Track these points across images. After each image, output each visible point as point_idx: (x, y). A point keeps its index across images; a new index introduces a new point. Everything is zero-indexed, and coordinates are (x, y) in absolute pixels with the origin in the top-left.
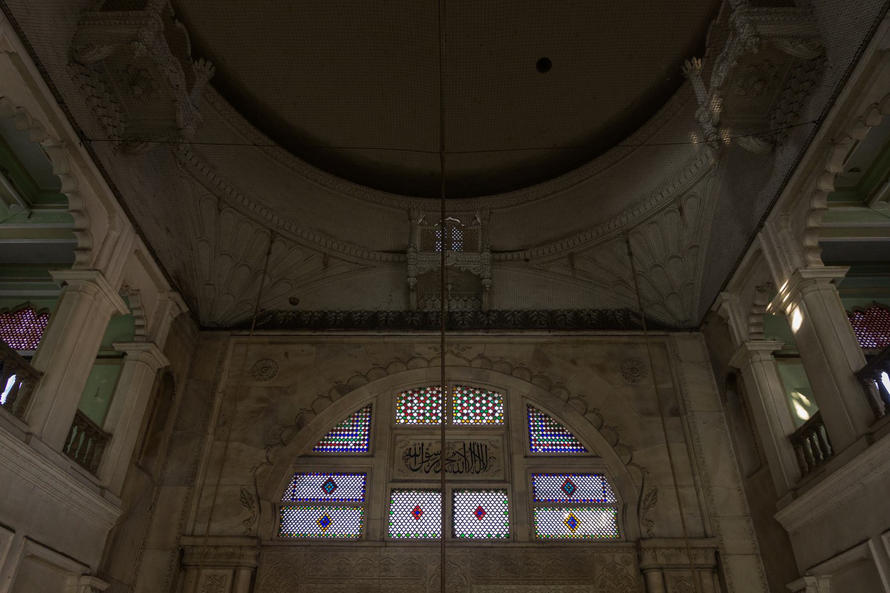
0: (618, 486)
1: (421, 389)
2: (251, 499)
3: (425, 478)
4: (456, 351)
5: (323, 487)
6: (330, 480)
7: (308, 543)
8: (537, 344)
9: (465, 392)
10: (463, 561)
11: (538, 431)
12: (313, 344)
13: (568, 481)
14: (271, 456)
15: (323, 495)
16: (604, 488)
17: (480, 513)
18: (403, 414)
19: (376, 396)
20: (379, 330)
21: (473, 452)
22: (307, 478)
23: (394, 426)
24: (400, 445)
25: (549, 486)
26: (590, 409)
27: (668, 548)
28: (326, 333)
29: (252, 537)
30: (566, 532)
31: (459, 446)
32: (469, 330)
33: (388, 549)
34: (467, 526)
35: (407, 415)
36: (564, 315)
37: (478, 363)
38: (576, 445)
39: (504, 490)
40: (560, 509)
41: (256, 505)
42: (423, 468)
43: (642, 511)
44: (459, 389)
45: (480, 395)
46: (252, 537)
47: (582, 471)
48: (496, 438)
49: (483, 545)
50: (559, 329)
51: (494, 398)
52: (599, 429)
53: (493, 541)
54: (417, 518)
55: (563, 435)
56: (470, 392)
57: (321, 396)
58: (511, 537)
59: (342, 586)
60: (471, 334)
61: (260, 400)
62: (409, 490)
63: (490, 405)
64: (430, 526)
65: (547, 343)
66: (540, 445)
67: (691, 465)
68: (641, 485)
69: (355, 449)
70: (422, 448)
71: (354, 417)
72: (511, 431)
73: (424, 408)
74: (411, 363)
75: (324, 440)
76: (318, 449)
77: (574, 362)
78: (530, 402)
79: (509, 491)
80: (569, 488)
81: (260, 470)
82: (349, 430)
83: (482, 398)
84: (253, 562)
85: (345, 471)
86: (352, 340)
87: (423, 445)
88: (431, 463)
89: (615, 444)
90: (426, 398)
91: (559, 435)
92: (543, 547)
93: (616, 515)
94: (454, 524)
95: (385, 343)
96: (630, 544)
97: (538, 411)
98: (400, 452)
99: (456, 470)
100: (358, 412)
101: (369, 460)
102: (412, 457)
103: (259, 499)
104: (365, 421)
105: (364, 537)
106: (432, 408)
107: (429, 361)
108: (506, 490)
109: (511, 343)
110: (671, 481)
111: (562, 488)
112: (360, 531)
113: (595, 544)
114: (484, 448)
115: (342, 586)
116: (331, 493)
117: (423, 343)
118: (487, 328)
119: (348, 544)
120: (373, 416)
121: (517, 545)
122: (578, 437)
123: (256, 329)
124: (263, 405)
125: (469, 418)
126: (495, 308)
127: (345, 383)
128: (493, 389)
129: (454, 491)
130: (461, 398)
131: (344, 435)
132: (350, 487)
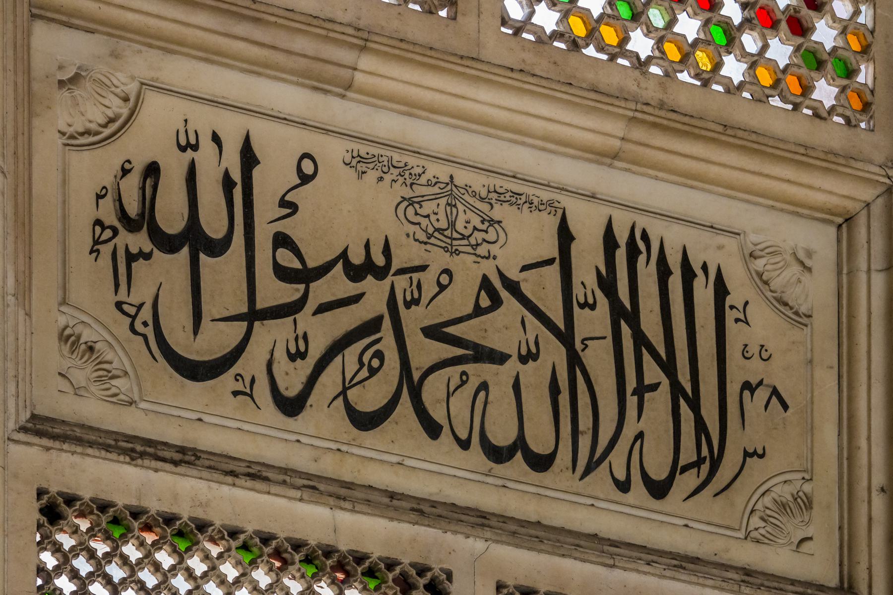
21: (624, 315)
24: (67, 113)
31: (524, 239)
42: (252, 364)
62: (183, 532)
70: (240, 186)
87: (249, 158)
88: (321, 331)
99: (502, 433)
102: (168, 243)
114: (704, 294)
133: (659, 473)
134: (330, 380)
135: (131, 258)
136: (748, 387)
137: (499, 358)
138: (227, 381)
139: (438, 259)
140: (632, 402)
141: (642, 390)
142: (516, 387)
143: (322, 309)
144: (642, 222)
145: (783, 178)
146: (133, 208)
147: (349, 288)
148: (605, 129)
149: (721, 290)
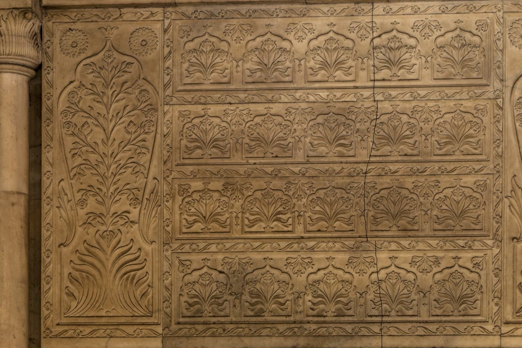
59: (276, 108)
84: (28, 51)
115: (276, 108)
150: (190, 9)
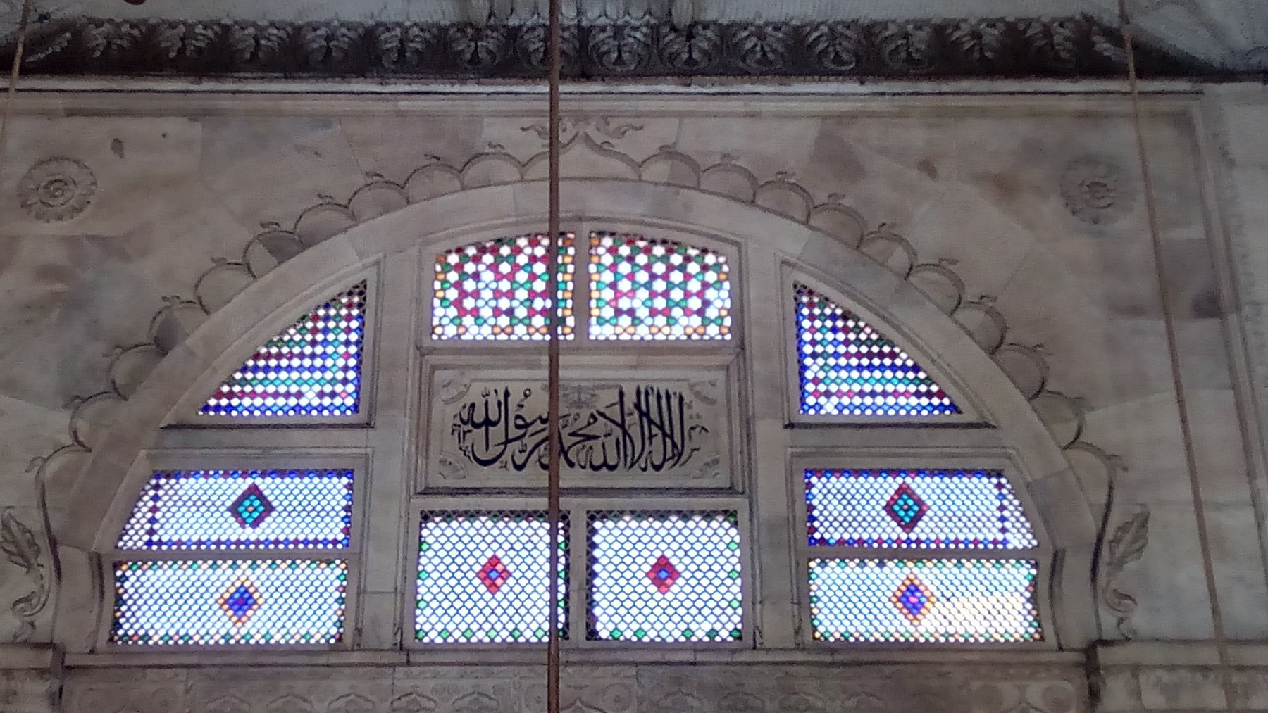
0: (1041, 505)
1: (500, 242)
2: (32, 543)
3: (513, 484)
4: (598, 138)
5: (234, 510)
6: (254, 490)
7: (193, 660)
8: (824, 117)
9: (625, 250)
10: (617, 700)
11: (824, 355)
12: (194, 116)
13: (903, 490)
14: (83, 426)
15: (233, 531)
16: (1002, 508)
17: (663, 573)
18: (453, 312)
19: (377, 263)
20: (383, 78)
21: (644, 414)
22: (188, 486)
23: (426, 343)
25: (850, 503)
26: (969, 296)
27: (1172, 668)
28: (229, 86)
29: (40, 646)
30: (894, 625)
32: (637, 76)
33: (415, 670)
34: (628, 608)
35: (463, 312)
36: (906, 36)
37: (659, 170)
38: (929, 395)
39: (729, 514)
40: (881, 565)
41: (46, 559)
42: (507, 457)
43: (1103, 569)
44: (608, 242)
45: (665, 259)
46: (40, 646)
47: (942, 464)
48: (708, 376)
49: (670, 657)
50: (891, 76)
51: (705, 268)
52: (993, 351)
53: (699, 647)
54: (493, 588)
55: (893, 368)
56: (640, 250)
57: (221, 263)
58: (747, 638)
60: (641, 88)
61: (47, 273)
63: (694, 286)
64: (526, 613)
65: (852, 116)
66: (828, 394)
67: (1247, 449)
68: (1104, 500)
69: (321, 408)
71: (316, 318)
72: (752, 360)
73: (510, 295)
74: (474, 171)
75: (231, 382)
76: (217, 408)
77: (928, 168)
78: (804, 279)
79: (743, 517)
80: (906, 510)
81: (53, 466)
82: (302, 356)
83: (671, 268)
85: (294, 465)
86: (308, 104)
87: (507, 394)
88: (530, 442)
89: (1037, 392)
90: (516, 268)
91: (882, 368)
92: (832, 664)
93: (1034, 581)
94: (591, 604)
95: (401, 114)
96: (1068, 657)
97: (826, 301)
98: (445, 414)
99: (597, 463)
100: (327, 306)
101: (361, 434)
102: (477, 426)
103: (54, 544)
104: (348, 330)
105: (348, 640)
106: (532, 295)
107: (523, 166)
108: (734, 514)
109: (752, 115)
110: (1186, 492)
111: (889, 508)
112: (340, 624)
113: (975, 657)
114: (675, 402)
116: (256, 524)
117: (502, 114)
118: (688, 71)
119: (305, 659)
120: (369, 317)
121: (762, 657)
122: (935, 373)
123: (25, 72)
124: (59, 287)
125: (636, 321)
126: (711, 15)
127: (288, 225)
128: (704, 242)
129: (593, 518)
130: (613, 267)
131: (289, 369)
132: (311, 506)
133: (657, 463)
134: (535, 456)
135: (465, 433)
136: (692, 428)
137: (596, 437)
138: (498, 464)
139: (574, 411)
140: (647, 442)
141: (651, 437)
142: (603, 445)
143: (532, 435)
144: (650, 384)
145: (696, 360)
146: (465, 418)
147: (543, 426)
148: (631, 359)
149: (681, 399)
150: (214, 671)
